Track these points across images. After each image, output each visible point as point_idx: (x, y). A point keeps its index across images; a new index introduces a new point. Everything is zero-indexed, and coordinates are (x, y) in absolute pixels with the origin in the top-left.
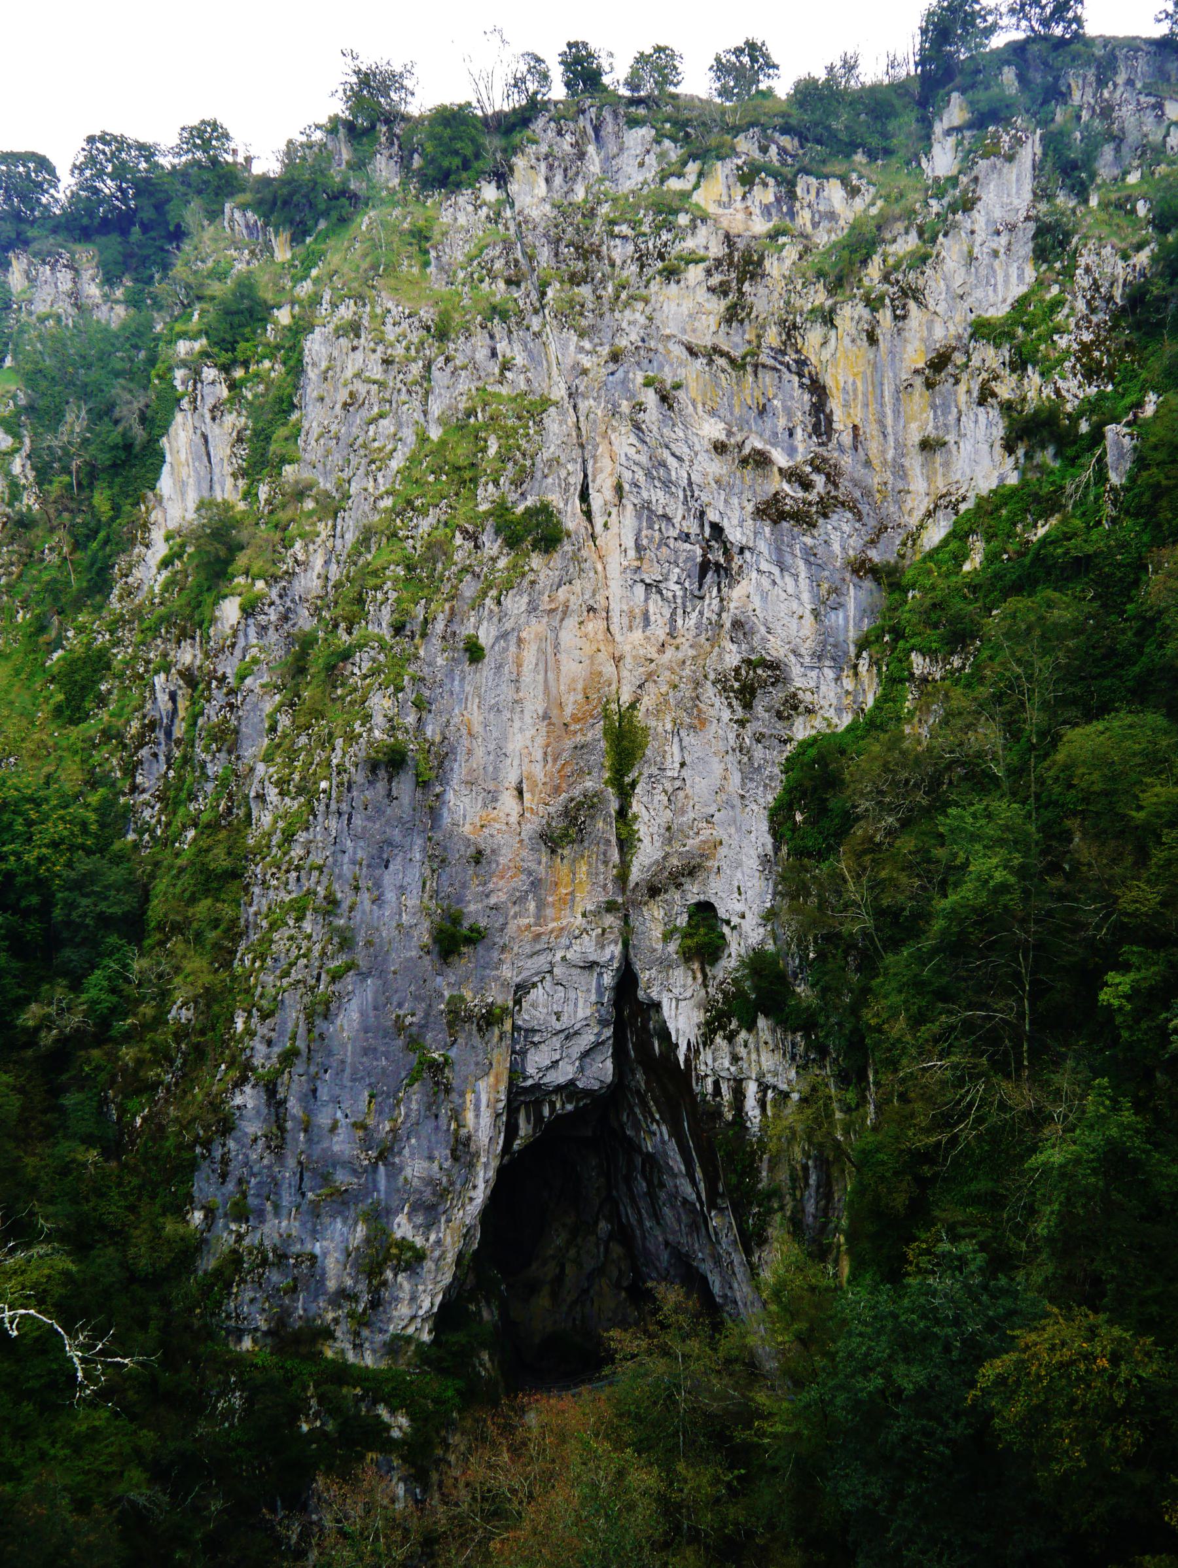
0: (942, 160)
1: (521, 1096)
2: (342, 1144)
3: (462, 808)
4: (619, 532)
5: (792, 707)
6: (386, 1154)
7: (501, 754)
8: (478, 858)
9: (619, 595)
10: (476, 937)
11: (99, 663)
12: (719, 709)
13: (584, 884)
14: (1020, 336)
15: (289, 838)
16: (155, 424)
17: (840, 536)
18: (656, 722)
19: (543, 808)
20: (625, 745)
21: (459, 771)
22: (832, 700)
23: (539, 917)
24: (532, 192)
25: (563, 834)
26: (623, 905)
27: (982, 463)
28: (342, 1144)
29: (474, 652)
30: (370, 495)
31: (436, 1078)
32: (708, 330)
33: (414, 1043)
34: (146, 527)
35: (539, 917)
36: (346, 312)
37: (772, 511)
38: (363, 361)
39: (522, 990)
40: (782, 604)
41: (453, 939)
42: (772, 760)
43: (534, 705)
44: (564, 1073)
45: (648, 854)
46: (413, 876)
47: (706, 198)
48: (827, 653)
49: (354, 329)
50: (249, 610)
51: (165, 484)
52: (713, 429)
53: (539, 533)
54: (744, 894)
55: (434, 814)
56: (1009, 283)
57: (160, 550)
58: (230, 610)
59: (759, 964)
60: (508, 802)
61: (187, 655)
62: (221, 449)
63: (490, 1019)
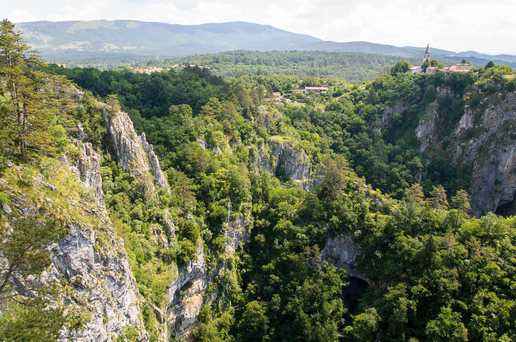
2: (480, 203)
3: (500, 168)
6: (485, 205)
7: (506, 162)
8: (501, 174)
10: (500, 183)
11: (449, 143)
15: (478, 170)
21: (500, 164)
23: (508, 181)
28: (480, 203)
29: (505, 151)
31: (493, 198)
33: (490, 193)
34: (457, 127)
35: (508, 181)
36: (492, 107)
39: (504, 189)
41: (497, 182)
43: (511, 157)
44: (507, 198)
46: (493, 176)
49: (493, 109)
50: (474, 142)
51: (460, 122)
55: (497, 169)
57: (459, 130)
58: (471, 141)
60: (506, 168)
62: (470, 119)
63: (500, 192)
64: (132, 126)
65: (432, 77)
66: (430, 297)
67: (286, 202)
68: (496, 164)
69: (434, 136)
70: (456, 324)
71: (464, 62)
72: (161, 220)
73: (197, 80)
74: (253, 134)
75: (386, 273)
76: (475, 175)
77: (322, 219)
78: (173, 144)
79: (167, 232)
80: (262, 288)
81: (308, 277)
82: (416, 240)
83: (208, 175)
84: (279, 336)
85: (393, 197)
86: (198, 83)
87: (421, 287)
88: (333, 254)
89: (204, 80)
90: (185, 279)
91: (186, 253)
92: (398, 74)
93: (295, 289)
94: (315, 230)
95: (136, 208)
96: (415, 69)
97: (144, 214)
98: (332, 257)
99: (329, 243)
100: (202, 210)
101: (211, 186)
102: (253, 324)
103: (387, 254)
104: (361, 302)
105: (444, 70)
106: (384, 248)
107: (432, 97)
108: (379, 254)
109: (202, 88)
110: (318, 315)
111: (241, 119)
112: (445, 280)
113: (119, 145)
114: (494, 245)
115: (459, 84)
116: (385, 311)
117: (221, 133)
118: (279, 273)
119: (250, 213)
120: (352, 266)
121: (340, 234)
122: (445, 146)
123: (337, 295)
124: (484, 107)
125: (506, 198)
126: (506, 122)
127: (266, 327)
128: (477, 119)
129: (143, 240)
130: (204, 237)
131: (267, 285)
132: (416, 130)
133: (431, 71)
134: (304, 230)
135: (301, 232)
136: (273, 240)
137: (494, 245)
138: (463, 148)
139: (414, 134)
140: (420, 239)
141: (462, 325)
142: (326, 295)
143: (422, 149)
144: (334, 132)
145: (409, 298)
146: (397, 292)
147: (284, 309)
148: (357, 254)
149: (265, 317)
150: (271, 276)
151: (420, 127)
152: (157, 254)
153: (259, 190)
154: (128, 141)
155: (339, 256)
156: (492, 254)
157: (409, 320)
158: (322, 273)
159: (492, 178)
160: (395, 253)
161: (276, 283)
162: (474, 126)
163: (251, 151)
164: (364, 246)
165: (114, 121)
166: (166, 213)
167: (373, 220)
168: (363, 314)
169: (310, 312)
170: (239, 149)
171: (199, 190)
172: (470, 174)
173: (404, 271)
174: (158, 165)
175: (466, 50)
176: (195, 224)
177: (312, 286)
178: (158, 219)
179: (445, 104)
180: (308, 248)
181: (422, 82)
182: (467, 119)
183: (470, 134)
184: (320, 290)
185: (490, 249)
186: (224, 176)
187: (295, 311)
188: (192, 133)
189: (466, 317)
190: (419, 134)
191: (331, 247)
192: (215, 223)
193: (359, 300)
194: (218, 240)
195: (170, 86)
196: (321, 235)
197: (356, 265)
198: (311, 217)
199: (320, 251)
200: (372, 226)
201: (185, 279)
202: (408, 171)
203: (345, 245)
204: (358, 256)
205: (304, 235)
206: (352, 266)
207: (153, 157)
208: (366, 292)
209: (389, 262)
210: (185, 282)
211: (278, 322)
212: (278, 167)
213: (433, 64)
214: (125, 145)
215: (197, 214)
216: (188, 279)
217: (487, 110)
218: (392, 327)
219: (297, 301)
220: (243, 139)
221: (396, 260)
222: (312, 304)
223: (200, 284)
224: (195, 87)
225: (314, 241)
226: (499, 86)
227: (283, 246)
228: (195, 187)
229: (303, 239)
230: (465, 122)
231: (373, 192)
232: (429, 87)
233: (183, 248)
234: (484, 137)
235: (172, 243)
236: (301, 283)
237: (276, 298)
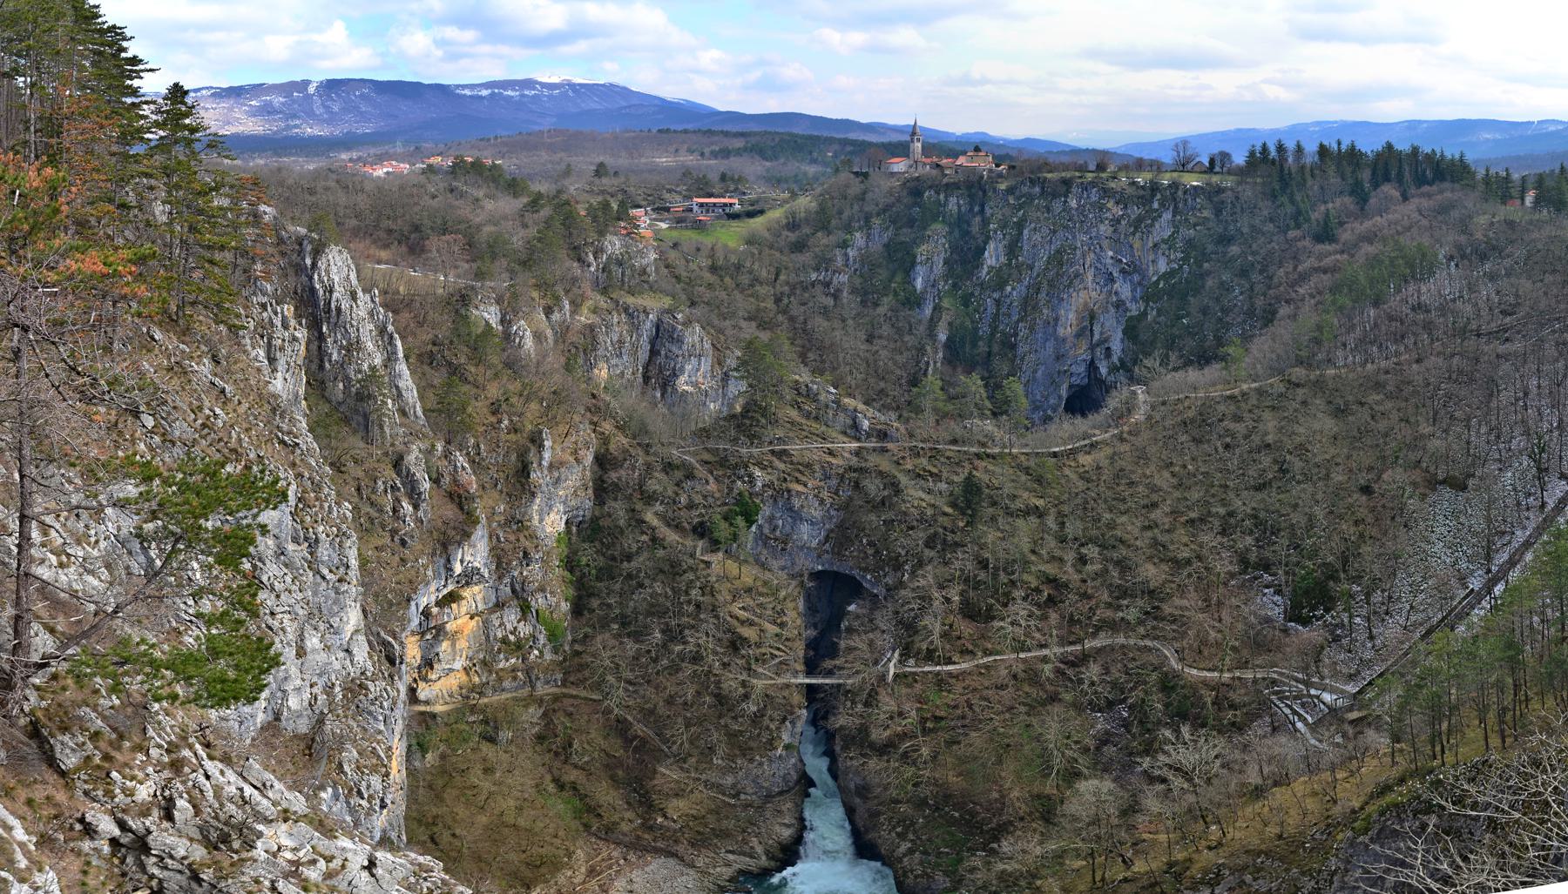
3: (1061, 331)
5: (1127, 310)
6: (1046, 399)
12: (1113, 310)
13: (1084, 345)
16: (986, 243)
17: (1136, 278)
20: (1092, 317)
22: (1134, 309)
26: (1092, 348)
30: (1040, 265)
37: (1123, 271)
38: (1037, 237)
40: (1124, 289)
41: (1059, 357)
45: (1096, 337)
47: (1109, 205)
48: (1134, 299)
52: (1111, 253)
58: (1009, 288)
62: (1001, 249)
71: (977, 149)
107: (936, 214)
113: (329, 311)
115: (975, 188)
124: (1020, 226)
125: (1076, 380)
126: (1058, 251)
128: (1013, 249)
138: (998, 302)
151: (918, 267)
154: (345, 305)
162: (1010, 260)
165: (322, 264)
172: (1013, 347)
175: (971, 130)
179: (960, 224)
182: (996, 249)
190: (919, 284)
207: (391, 337)
214: (339, 310)
217: (1026, 232)
226: (1037, 189)
230: (993, 256)
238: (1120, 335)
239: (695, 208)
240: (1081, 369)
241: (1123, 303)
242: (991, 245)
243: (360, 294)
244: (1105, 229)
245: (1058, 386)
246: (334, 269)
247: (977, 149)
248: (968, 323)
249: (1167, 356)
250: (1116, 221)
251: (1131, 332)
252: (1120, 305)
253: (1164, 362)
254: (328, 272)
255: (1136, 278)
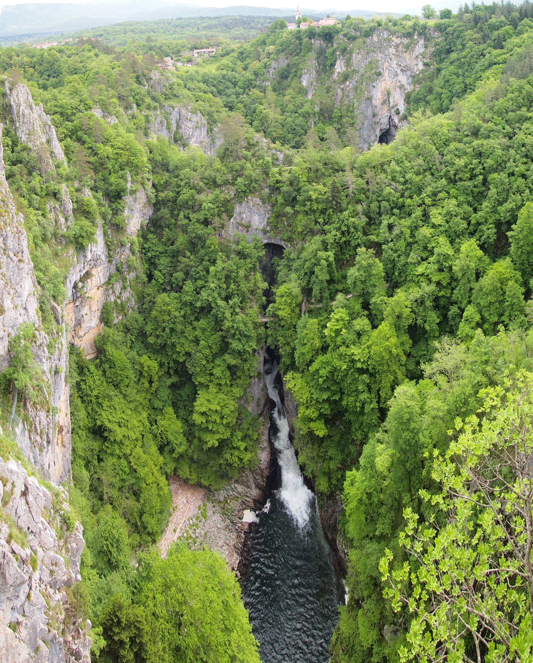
0: (416, 37)
1: (381, 130)
4: (386, 73)
5: (405, 89)
9: (387, 78)
12: (398, 90)
13: (386, 108)
14: (423, 55)
17: (409, 73)
18: (392, 91)
19: (381, 101)
20: (389, 94)
22: (409, 88)
24: (375, 39)
25: (384, 103)
27: (421, 67)
30: (362, 71)
32: (394, 52)
37: (402, 70)
40: (403, 79)
42: (404, 95)
45: (392, 104)
47: (393, 39)
53: (379, 74)
54: (402, 108)
56: (422, 50)
58: (348, 83)
59: (404, 114)
61: (342, 86)
64: (30, 98)
65: (306, 31)
66: (345, 242)
67: (188, 170)
68: (369, 99)
69: (317, 82)
70: (372, 262)
72: (58, 196)
73: (90, 51)
74: (148, 100)
75: (299, 230)
76: (357, 112)
77: (226, 183)
78: (69, 113)
79: (64, 212)
80: (171, 275)
81: (220, 254)
82: (320, 187)
83: (105, 145)
84: (196, 337)
85: (294, 147)
86: (91, 54)
87: (334, 233)
88: (243, 222)
89: (97, 50)
90: (84, 268)
91: (84, 234)
92: (278, 31)
93: (208, 272)
94: (222, 197)
95: (33, 182)
96: (292, 27)
97: (42, 188)
98: (242, 225)
99: (238, 209)
100: (101, 184)
101: (108, 157)
102: (164, 325)
103: (297, 207)
104: (280, 271)
105: (314, 24)
106: (293, 201)
108: (288, 209)
109: (95, 58)
110: (236, 300)
111: (135, 86)
112: (353, 219)
114: (385, 171)
115: (328, 36)
116: (306, 274)
117: (115, 100)
118: (188, 254)
119: (151, 185)
120: (265, 232)
121: (247, 197)
122: (328, 90)
123: (254, 269)
126: (370, 63)
127: (179, 327)
128: (348, 63)
129: (40, 218)
130: (104, 216)
131: (176, 272)
132: (302, 79)
133: (304, 27)
134: (211, 197)
135: (206, 199)
136: (178, 215)
137: (385, 171)
138: (342, 89)
139: (300, 83)
140: (324, 185)
141: (377, 260)
142: (242, 273)
143: (310, 97)
144: (227, 91)
145: (326, 250)
146: (315, 247)
147: (198, 300)
148: (267, 216)
149: (177, 314)
150: (179, 258)
151: (304, 76)
152: (55, 235)
153: (159, 158)
155: (250, 222)
156: (385, 181)
157: (330, 276)
158: (234, 246)
159: (369, 113)
160: (305, 205)
161: (186, 266)
163: (147, 117)
164: (274, 205)
166: (64, 188)
167: (277, 175)
168: (285, 285)
169: (227, 299)
170: (134, 117)
171: (96, 162)
173: (316, 222)
174: (55, 136)
176: (94, 202)
177: (226, 265)
178: (55, 195)
179: (321, 53)
180: (217, 219)
181: (298, 36)
183: (346, 77)
184: (235, 268)
185: (383, 176)
186: (122, 146)
187: (210, 299)
188: (87, 102)
189: (377, 248)
190: (305, 83)
191: (240, 214)
192: (115, 196)
193: (279, 268)
194: (118, 219)
195: (65, 58)
196: (228, 201)
197: (268, 229)
198: (215, 182)
199: (230, 219)
200: (278, 182)
201: (84, 268)
202: (301, 118)
203: (254, 209)
204: (269, 219)
205: (211, 205)
206: (265, 232)
208: (283, 258)
209: (300, 217)
210: (84, 272)
211: (192, 318)
212: (176, 133)
213: (305, 20)
215: (95, 189)
216: (87, 268)
218: (316, 291)
219: (212, 285)
220: (138, 105)
221: (306, 213)
222: (228, 288)
223: (101, 275)
224: (88, 58)
225: (223, 209)
227: (190, 220)
228: (92, 159)
229: (209, 209)
230: (340, 67)
231: (273, 145)
232: (305, 40)
233: (82, 228)
234: (356, 77)
235: (69, 223)
236: (213, 262)
237: (189, 287)
238: (403, 102)
239: (196, 55)
240: (385, 120)
241: (403, 86)
242: (338, 63)
243: (34, 106)
244: (392, 50)
245: (374, 129)
246: (20, 94)
247: (328, 17)
248: (329, 101)
249: (425, 111)
250: (397, 46)
251: (408, 99)
252: (402, 87)
253: (424, 112)
254: (17, 96)
255: (409, 73)
